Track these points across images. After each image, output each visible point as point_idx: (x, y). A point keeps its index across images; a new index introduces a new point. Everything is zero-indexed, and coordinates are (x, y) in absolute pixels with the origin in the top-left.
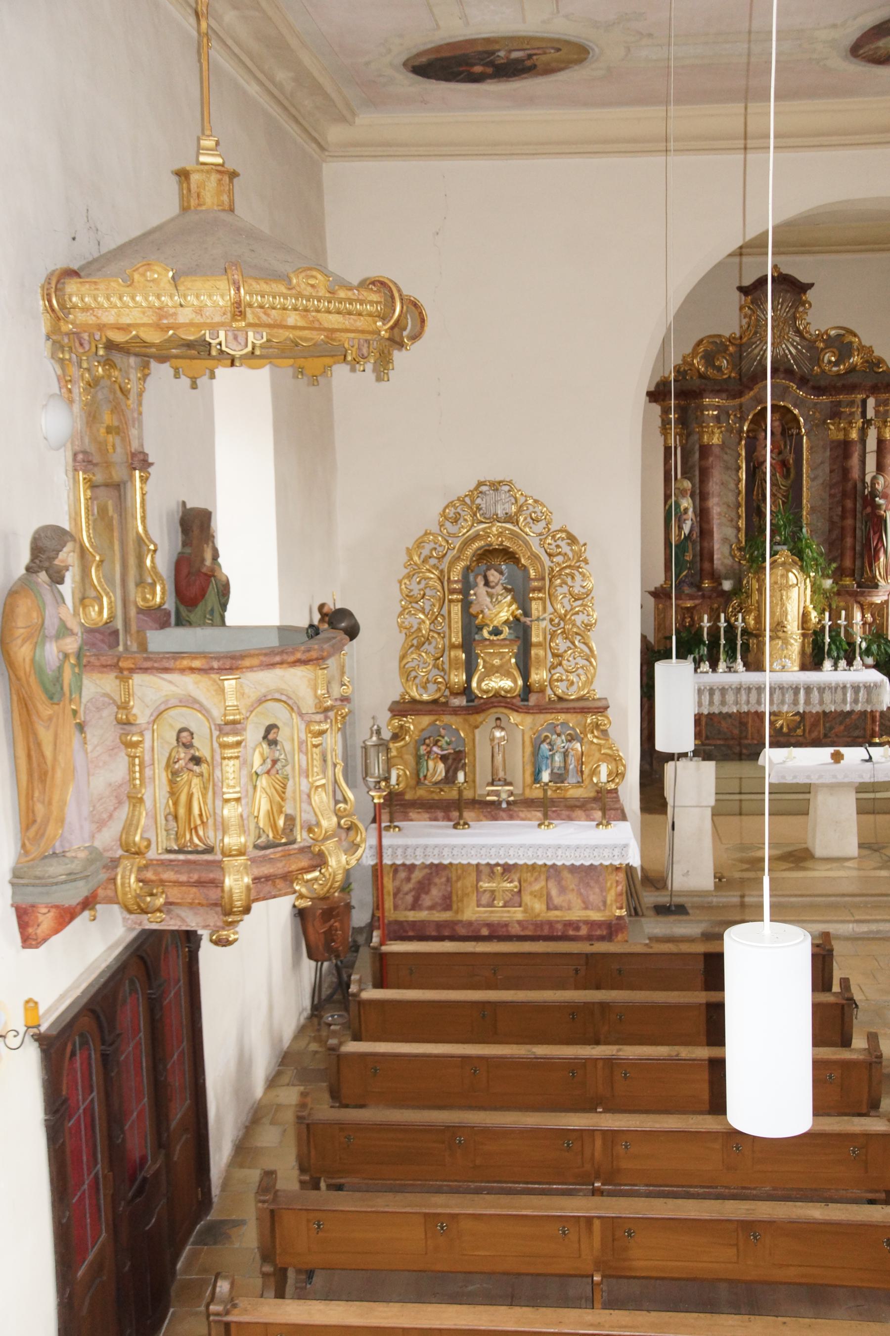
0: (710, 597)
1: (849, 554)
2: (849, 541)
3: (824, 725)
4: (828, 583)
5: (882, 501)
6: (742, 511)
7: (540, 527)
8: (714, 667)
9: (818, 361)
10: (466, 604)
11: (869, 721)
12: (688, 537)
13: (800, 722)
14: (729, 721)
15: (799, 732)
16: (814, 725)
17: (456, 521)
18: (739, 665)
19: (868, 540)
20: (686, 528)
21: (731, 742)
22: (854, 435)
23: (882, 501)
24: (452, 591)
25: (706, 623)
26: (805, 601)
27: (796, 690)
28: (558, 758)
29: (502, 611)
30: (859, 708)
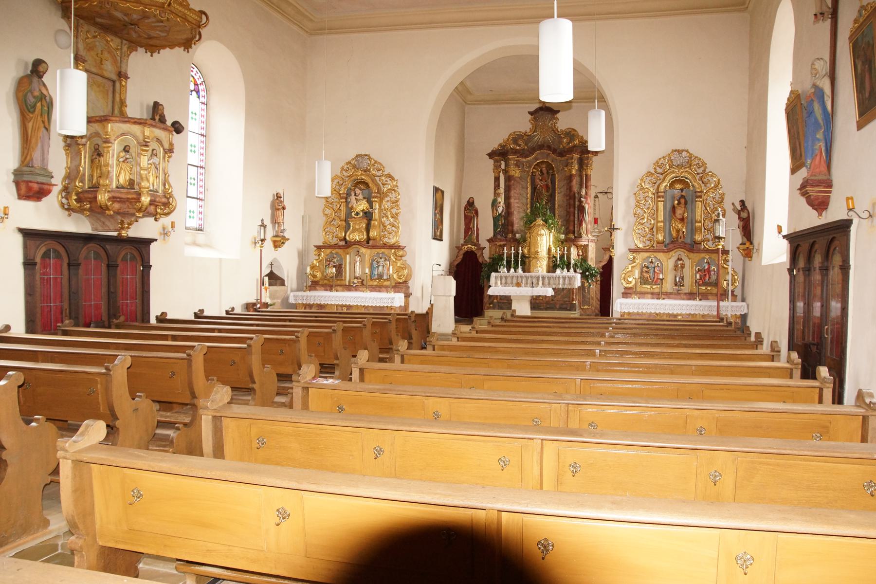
2: (572, 218)
4: (563, 236)
6: (529, 206)
7: (379, 174)
8: (509, 271)
9: (561, 142)
10: (347, 203)
12: (500, 215)
17: (346, 171)
18: (520, 270)
20: (500, 210)
24: (342, 198)
25: (505, 251)
27: (538, 278)
28: (381, 268)
29: (363, 206)
30: (565, 287)
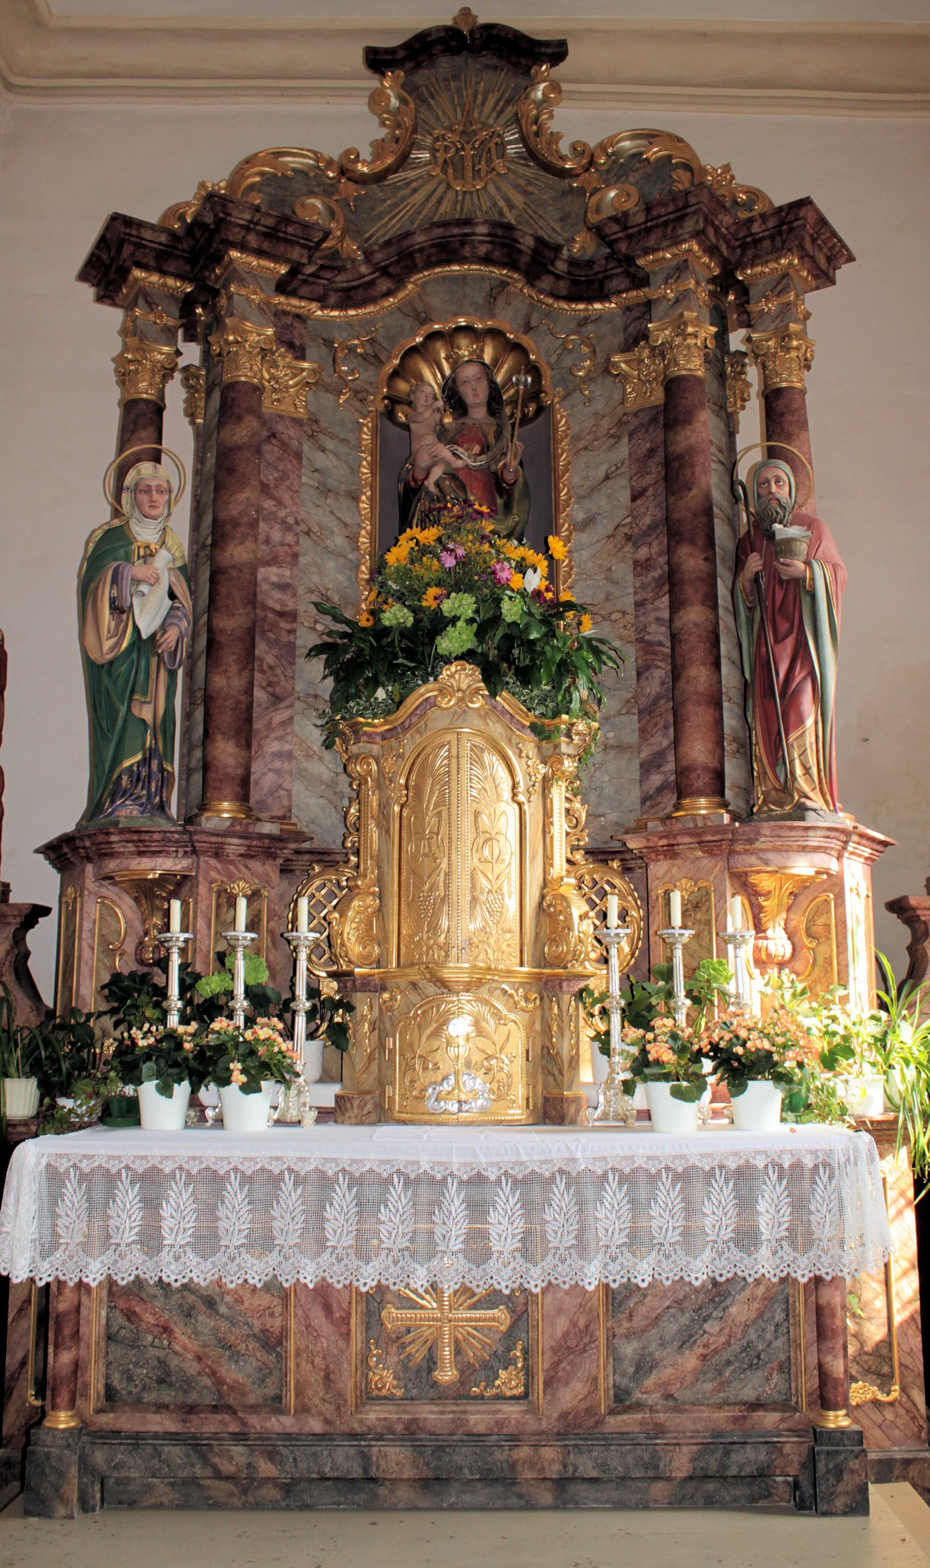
0: (218, 853)
1: (698, 717)
3: (612, 1350)
5: (794, 531)
11: (806, 1332)
13: (510, 1336)
14: (205, 1321)
15: (508, 1380)
16: (572, 1347)
19: (764, 666)
21: (210, 1425)
22: (693, 365)
23: (794, 531)
26: (548, 860)
